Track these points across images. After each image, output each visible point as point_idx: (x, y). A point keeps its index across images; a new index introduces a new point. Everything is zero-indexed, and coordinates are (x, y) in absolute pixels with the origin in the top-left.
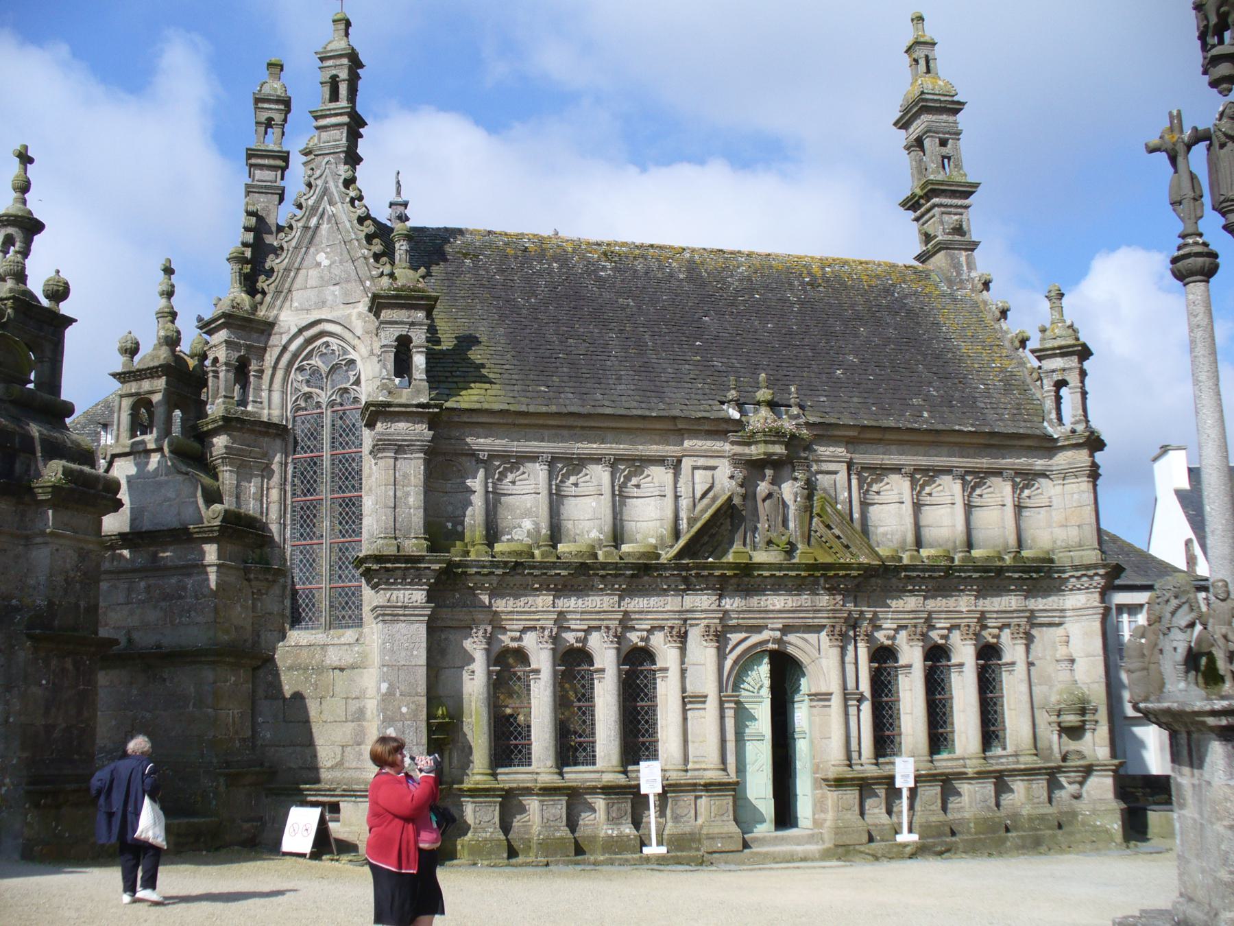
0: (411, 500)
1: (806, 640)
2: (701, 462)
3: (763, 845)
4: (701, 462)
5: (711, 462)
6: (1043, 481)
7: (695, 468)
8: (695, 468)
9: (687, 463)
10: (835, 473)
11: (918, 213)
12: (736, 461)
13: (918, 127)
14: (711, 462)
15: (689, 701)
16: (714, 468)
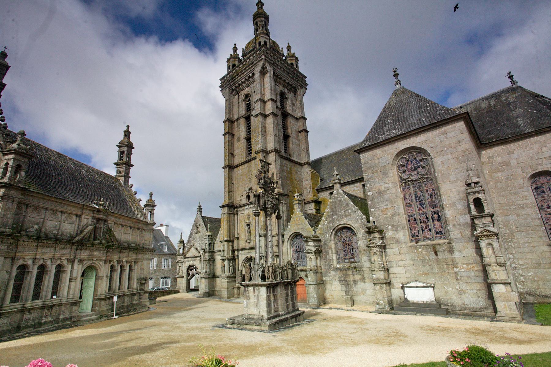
0: (9, 216)
1: (99, 263)
2: (86, 217)
3: (83, 318)
4: (86, 217)
5: (88, 217)
6: (143, 231)
7: (84, 218)
8: (84, 218)
9: (83, 216)
10: (111, 224)
11: (118, 167)
12: (93, 218)
13: (122, 149)
14: (88, 217)
15: (71, 280)
16: (88, 219)
